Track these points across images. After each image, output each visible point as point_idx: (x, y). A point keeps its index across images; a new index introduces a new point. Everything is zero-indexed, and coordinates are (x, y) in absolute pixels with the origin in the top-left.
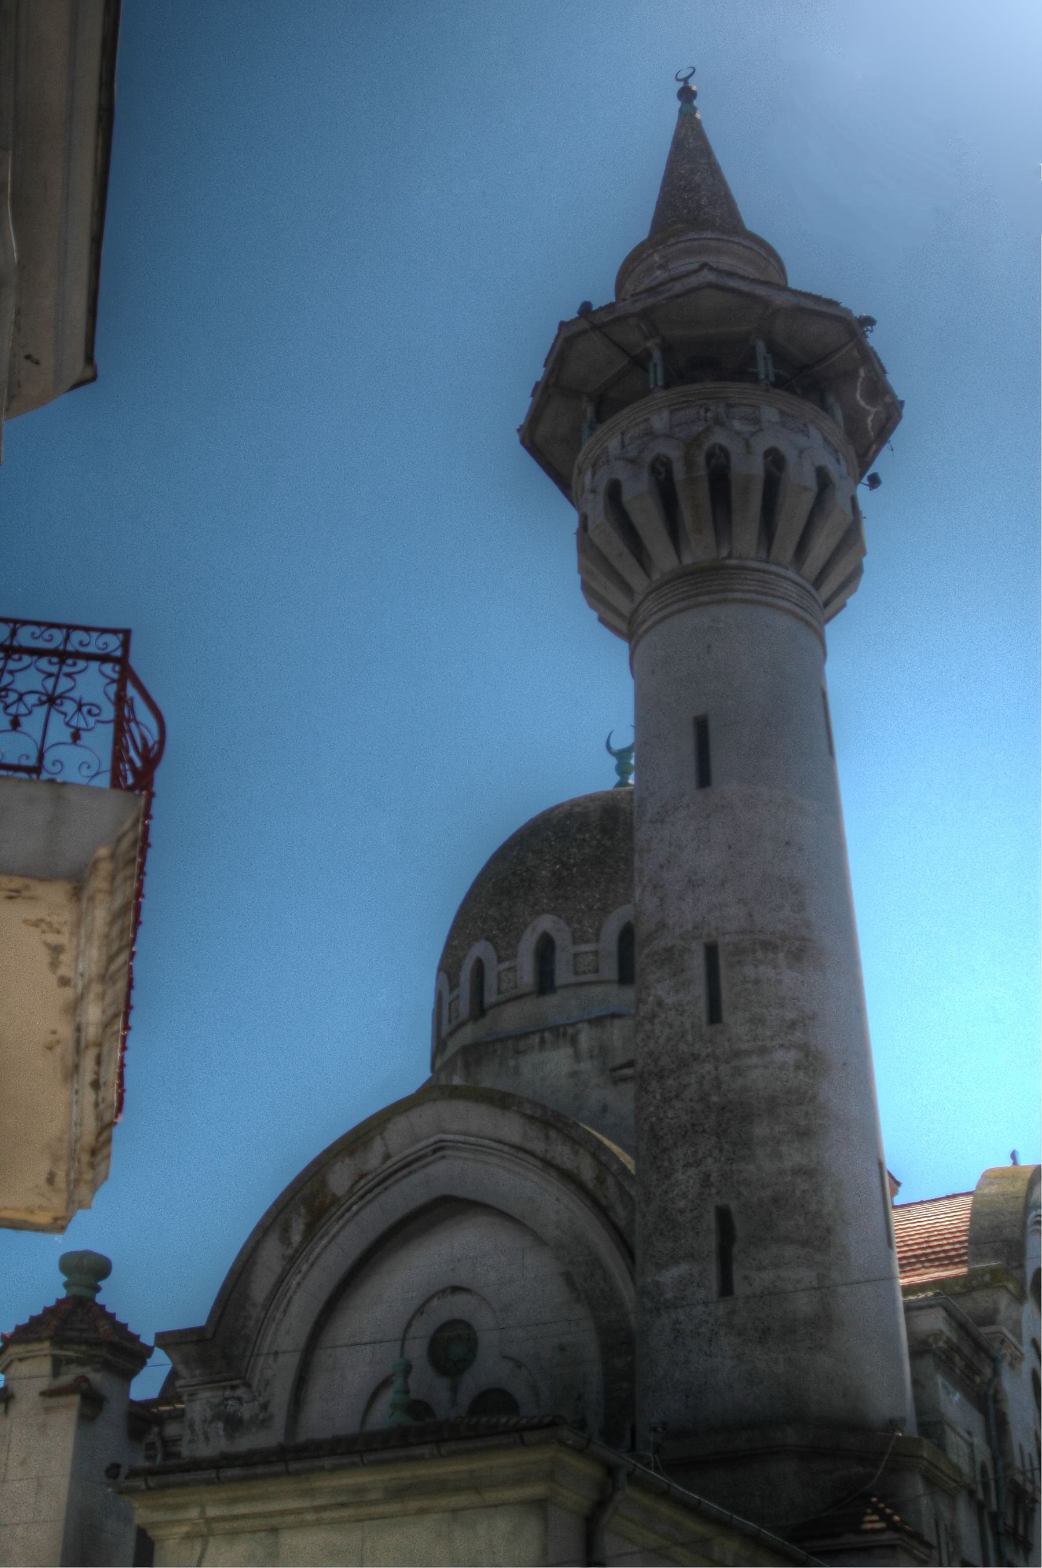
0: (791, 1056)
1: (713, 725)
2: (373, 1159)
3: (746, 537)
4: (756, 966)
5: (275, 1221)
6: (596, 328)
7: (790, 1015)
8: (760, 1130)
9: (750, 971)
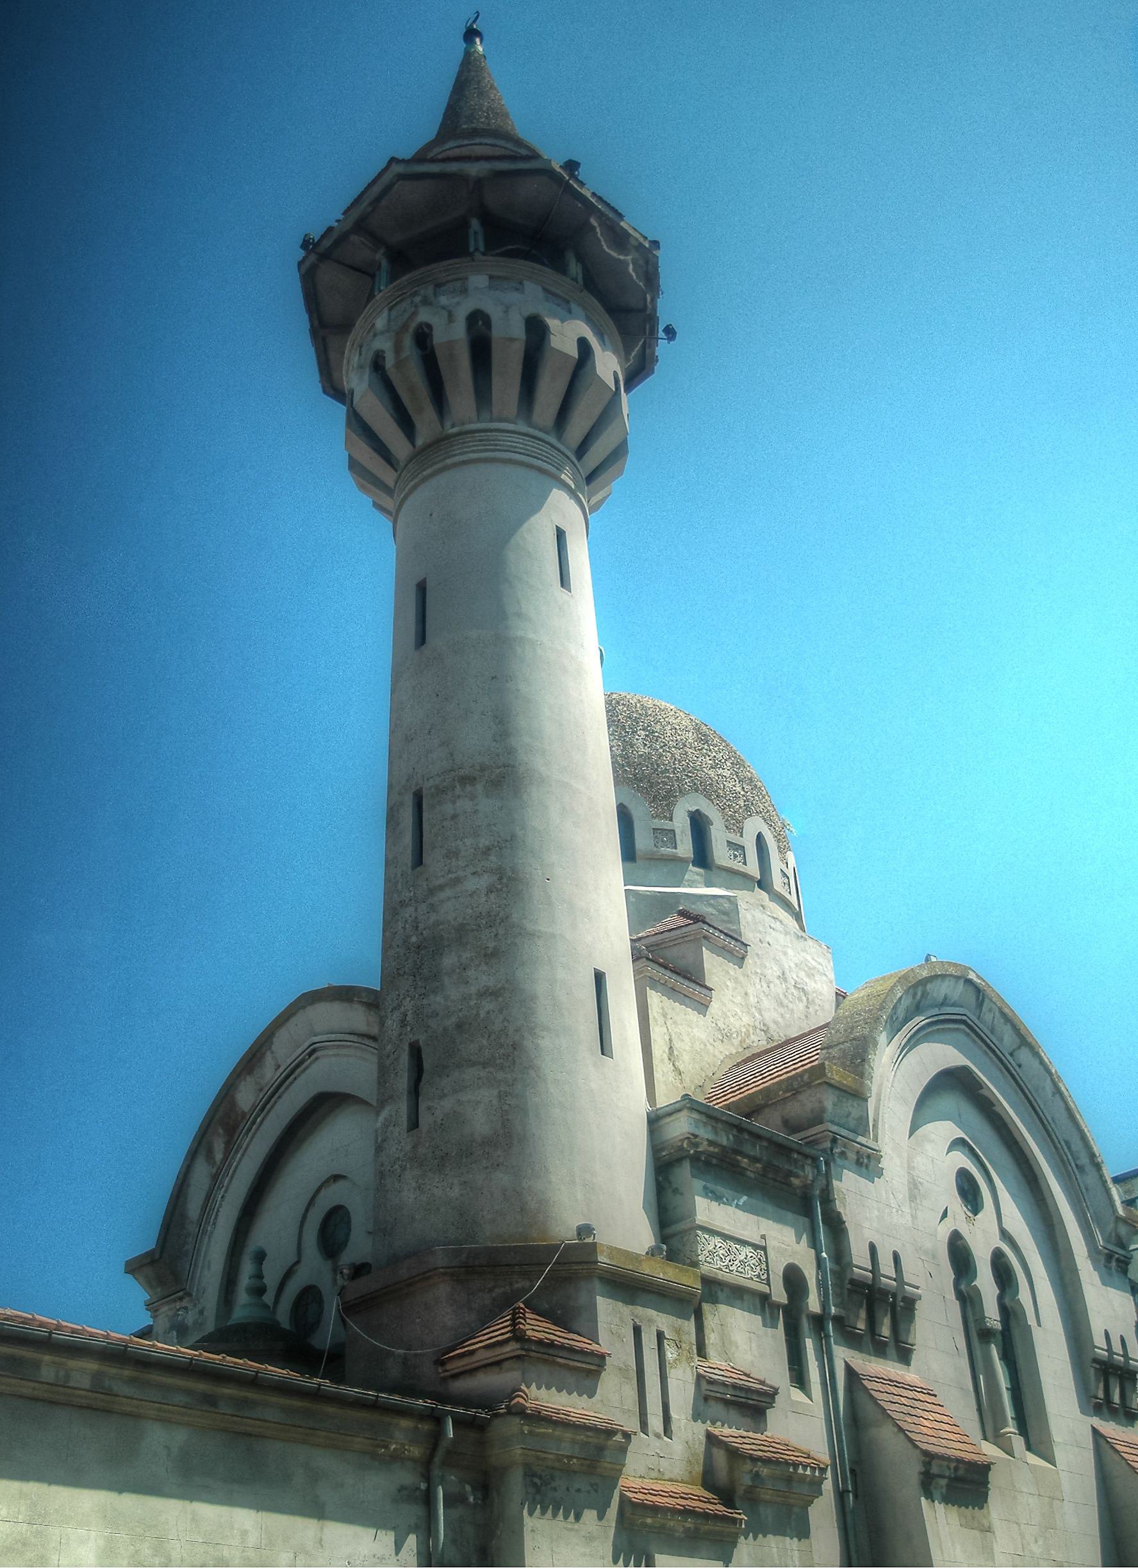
0: (485, 881)
1: (430, 585)
2: (269, 1073)
3: (462, 399)
4: (454, 803)
5: (200, 1146)
6: (324, 256)
7: (484, 842)
8: (449, 961)
9: (448, 809)
